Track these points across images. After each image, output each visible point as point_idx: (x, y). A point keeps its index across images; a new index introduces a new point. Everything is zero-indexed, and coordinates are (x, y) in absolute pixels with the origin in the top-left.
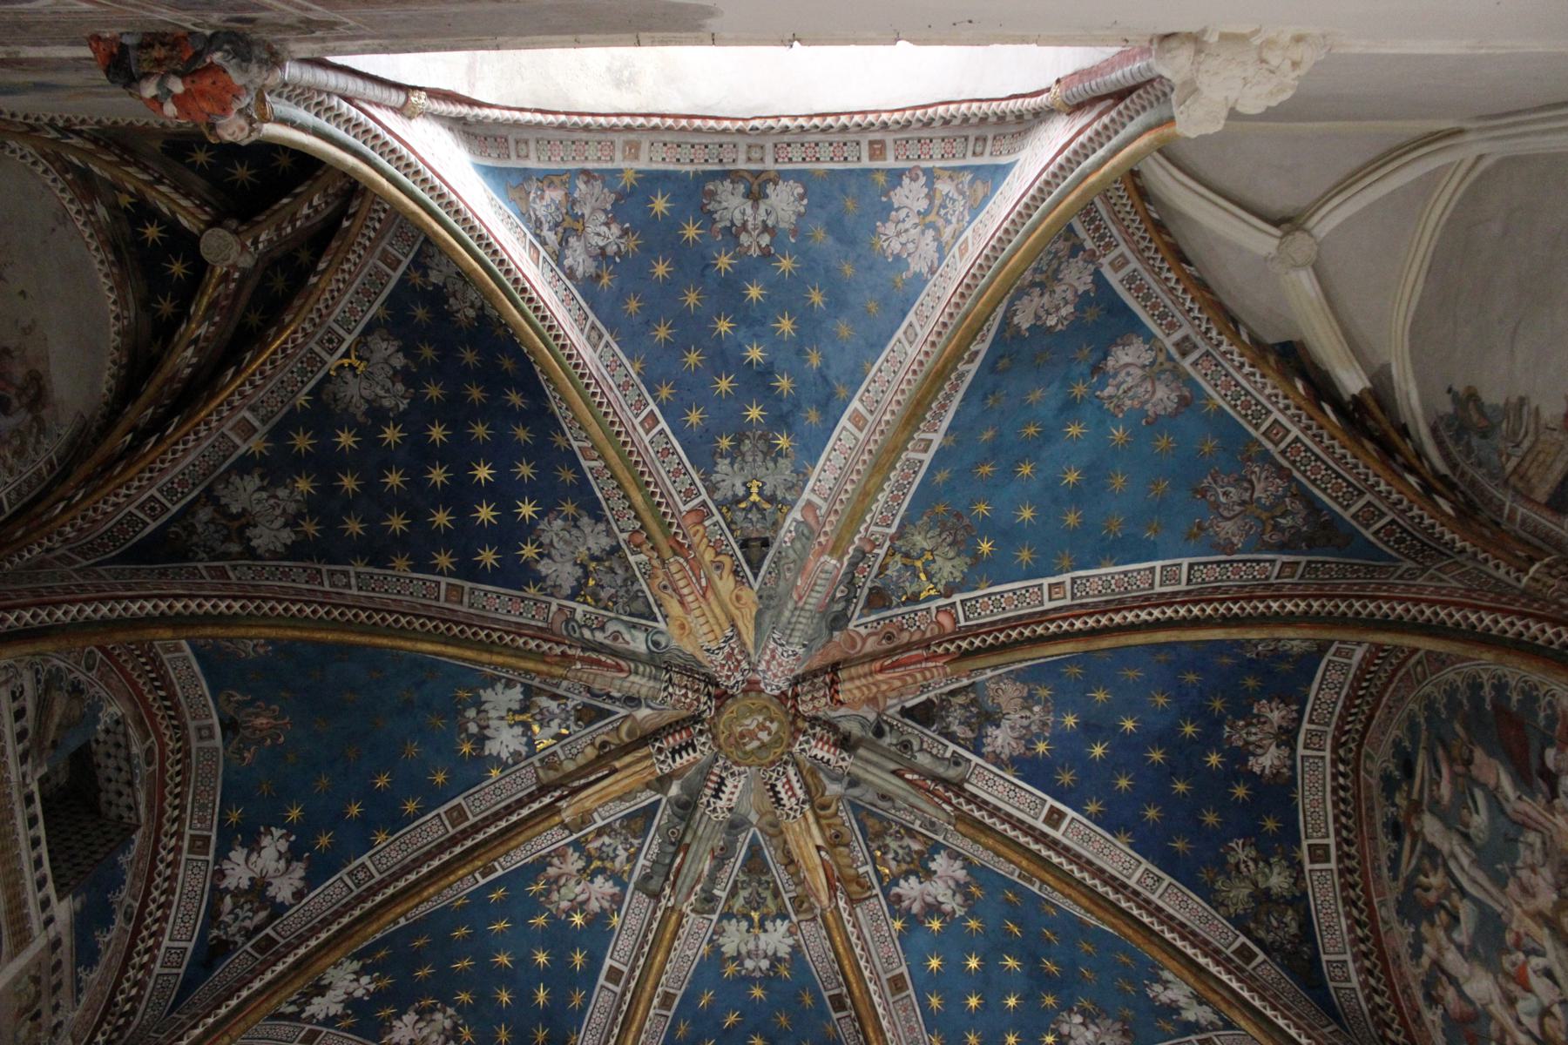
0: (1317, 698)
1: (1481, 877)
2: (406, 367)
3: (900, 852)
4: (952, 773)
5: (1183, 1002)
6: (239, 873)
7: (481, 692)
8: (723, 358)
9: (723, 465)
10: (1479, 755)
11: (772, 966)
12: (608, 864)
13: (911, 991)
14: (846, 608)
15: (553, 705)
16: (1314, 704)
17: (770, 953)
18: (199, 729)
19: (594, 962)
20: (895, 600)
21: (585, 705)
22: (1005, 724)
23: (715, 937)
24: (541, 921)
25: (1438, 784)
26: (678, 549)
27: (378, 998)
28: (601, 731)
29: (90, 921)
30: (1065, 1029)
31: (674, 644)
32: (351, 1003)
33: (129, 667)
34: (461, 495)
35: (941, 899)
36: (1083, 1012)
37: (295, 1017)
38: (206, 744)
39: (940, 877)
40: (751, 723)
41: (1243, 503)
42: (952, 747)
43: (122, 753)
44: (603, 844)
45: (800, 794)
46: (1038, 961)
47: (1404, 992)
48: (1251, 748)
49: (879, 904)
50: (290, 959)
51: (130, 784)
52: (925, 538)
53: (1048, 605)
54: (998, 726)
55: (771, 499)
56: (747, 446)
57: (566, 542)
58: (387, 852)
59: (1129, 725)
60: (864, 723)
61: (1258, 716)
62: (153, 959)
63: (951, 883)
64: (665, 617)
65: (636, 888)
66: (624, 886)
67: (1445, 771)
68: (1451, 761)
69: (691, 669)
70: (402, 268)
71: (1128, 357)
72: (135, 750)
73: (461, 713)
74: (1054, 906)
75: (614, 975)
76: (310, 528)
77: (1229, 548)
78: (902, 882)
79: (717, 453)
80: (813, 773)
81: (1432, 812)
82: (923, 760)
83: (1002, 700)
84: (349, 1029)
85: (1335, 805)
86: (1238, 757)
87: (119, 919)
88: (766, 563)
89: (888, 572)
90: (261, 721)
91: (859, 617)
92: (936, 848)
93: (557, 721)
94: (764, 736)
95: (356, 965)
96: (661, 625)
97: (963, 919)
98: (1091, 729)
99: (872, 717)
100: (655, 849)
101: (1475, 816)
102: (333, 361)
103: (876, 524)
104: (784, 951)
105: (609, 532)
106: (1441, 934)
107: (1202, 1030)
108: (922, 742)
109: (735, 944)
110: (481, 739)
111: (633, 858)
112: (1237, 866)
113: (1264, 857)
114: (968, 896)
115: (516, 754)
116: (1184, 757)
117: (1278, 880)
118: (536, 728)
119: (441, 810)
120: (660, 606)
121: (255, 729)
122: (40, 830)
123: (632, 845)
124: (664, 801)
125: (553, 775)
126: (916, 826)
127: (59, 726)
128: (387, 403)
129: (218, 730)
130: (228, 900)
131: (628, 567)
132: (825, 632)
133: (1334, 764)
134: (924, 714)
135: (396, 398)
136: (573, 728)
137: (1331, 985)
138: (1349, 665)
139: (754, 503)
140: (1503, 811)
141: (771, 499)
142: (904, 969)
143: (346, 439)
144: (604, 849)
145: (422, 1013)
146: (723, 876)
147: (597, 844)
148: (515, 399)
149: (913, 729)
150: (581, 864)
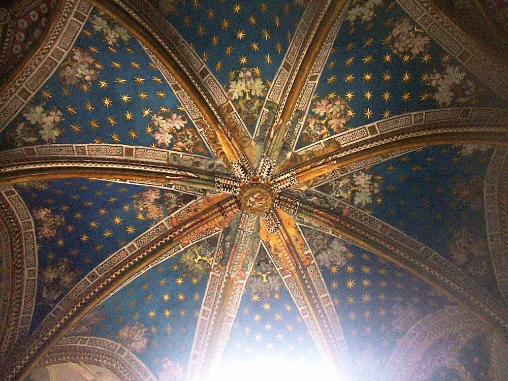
0: (33, 244)
3: (186, 139)
7: (371, 202)
11: (237, 75)
12: (318, 121)
14: (225, 237)
15: (342, 194)
16: (33, 241)
17: (240, 81)
20: (206, 242)
21: (328, 193)
22: (153, 201)
23: (266, 89)
30: (92, 72)
31: (292, 217)
32: (442, 70)
35: (164, 121)
36: (86, 82)
39: (167, 131)
42: (173, 189)
44: (320, 131)
48: (51, 216)
52: (198, 268)
54: (155, 199)
55: (258, 276)
57: (335, 256)
63: (161, 130)
64: (296, 227)
65: (304, 113)
66: (310, 112)
73: (381, 192)
78: (183, 126)
86: (55, 212)
88: (258, 252)
89: (210, 254)
90: (466, 193)
91: (219, 234)
92: (171, 147)
93: (340, 186)
96: (297, 224)
103: (218, 278)
108: (186, 189)
109: (257, 84)
110: (373, 180)
111: (307, 124)
114: (153, 126)
120: (299, 232)
123: (307, 131)
124: (294, 149)
126: (181, 154)
128: (400, 308)
129: (485, 190)
131: (311, 247)
136: (333, 183)
138: (28, 267)
139: (264, 274)
141: (258, 276)
142: (175, 93)
144: (320, 129)
147: (322, 131)
150: (330, 122)
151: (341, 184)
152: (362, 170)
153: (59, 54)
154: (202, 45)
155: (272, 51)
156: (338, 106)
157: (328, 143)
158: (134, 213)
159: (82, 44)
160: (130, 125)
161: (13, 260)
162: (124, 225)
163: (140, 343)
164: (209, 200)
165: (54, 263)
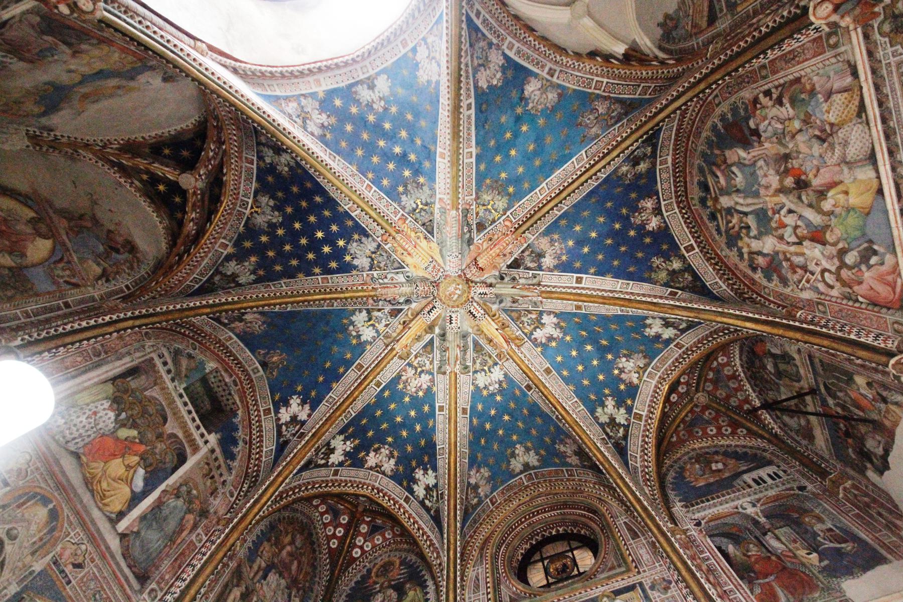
1: (749, 201)
2: (275, 204)
4: (535, 281)
5: (660, 331)
6: (285, 415)
8: (387, 156)
9: (404, 198)
10: (728, 153)
11: (500, 385)
13: (554, 372)
15: (379, 314)
18: (253, 370)
19: (432, 407)
22: (547, 255)
24: (407, 399)
25: (719, 182)
26: (398, 232)
27: (357, 449)
28: (401, 317)
29: (228, 443)
30: (621, 366)
31: (414, 275)
32: (346, 454)
33: (212, 347)
34: (315, 245)
36: (625, 356)
37: (326, 465)
38: (257, 375)
40: (451, 289)
41: (596, 118)
42: (531, 272)
43: (223, 383)
45: (482, 312)
46: (598, 342)
47: (744, 276)
49: (529, 344)
50: (310, 434)
51: (230, 394)
53: (541, 197)
55: (427, 204)
56: (409, 187)
58: (338, 391)
59: (594, 235)
60: (495, 277)
61: (642, 208)
62: (261, 456)
66: (432, 374)
67: (719, 174)
68: (718, 166)
69: (424, 280)
70: (255, 162)
71: (532, 88)
72: (227, 380)
73: (347, 329)
74: (594, 315)
75: (441, 409)
76: (261, 273)
77: (597, 136)
79: (399, 194)
80: (485, 305)
81: (721, 195)
82: (522, 281)
83: (542, 246)
84: (350, 466)
85: (688, 227)
86: (642, 226)
87: (241, 443)
90: (275, 359)
92: (541, 313)
94: (458, 292)
95: (342, 437)
96: (407, 269)
97: (563, 338)
98: (580, 243)
99: (497, 274)
100: (439, 356)
101: (737, 179)
102: (248, 212)
104: (502, 378)
105: (374, 240)
106: (746, 239)
107: (674, 340)
110: (359, 336)
111: (432, 363)
112: (658, 267)
113: (667, 259)
114: (561, 328)
115: (374, 338)
116: (620, 237)
117: (676, 265)
118: (377, 325)
119: (353, 367)
121: (273, 363)
122: (190, 407)
125: (389, 340)
126: (530, 308)
127: (187, 369)
128: (274, 221)
130: (284, 427)
131: (386, 252)
132: (467, 248)
133: (680, 212)
134: (516, 264)
135: (277, 218)
137: (714, 292)
140: (745, 165)
141: (427, 204)
143: (264, 239)
145: (376, 451)
146: (468, 356)
147: (417, 361)
148: (318, 199)
149: (514, 272)
150: (414, 372)
151: (384, 322)
152: (371, 343)
153: (650, 375)
154: (534, 410)
155: (480, 415)
156: (412, 389)
157: (408, 355)
158: (564, 239)
159: (633, 390)
160: (581, 327)
161: (685, 178)
162: (570, 227)
163: (531, 89)
164: (495, 267)
165: (638, 176)
